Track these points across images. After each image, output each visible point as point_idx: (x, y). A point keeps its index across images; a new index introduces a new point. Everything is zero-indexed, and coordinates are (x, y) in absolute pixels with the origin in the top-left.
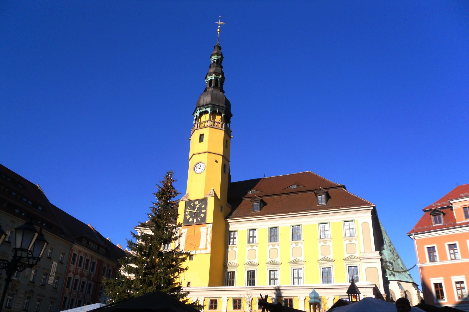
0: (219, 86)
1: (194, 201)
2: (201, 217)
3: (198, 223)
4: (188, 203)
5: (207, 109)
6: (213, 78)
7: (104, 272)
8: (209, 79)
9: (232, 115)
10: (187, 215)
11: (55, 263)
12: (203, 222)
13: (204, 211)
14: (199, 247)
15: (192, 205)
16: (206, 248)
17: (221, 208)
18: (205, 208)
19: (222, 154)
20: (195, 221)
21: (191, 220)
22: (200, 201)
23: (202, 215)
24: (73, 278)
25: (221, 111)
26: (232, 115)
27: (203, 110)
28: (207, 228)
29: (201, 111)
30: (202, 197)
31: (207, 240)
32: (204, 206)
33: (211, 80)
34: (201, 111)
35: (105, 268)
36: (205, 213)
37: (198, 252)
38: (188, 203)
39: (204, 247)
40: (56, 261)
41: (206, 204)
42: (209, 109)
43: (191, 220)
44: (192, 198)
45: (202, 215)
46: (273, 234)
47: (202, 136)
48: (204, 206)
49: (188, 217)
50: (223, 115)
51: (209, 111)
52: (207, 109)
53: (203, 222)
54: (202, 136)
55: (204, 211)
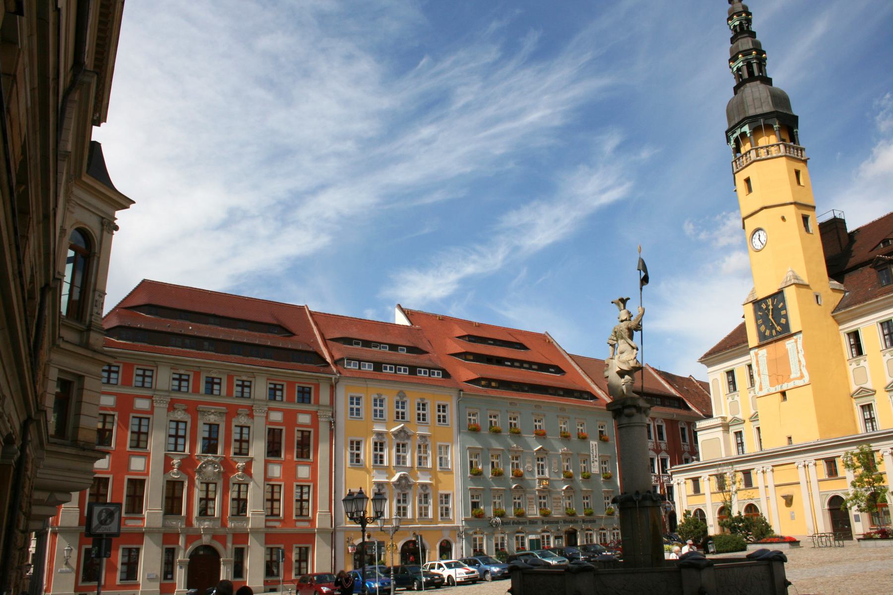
0: (756, 74)
3: (780, 336)
5: (743, 130)
7: (684, 436)
9: (797, 117)
11: (593, 443)
12: (785, 333)
13: (783, 312)
14: (792, 376)
15: (764, 306)
16: (802, 377)
17: (817, 297)
20: (774, 332)
21: (767, 333)
25: (770, 122)
26: (797, 117)
28: (796, 342)
29: (735, 135)
31: (799, 361)
34: (735, 135)
35: (683, 429)
39: (799, 375)
40: (594, 440)
41: (783, 300)
42: (746, 129)
43: (767, 333)
44: (760, 297)
45: (783, 321)
47: (748, 181)
49: (763, 328)
50: (776, 126)
51: (748, 131)
52: (743, 130)
54: (748, 181)
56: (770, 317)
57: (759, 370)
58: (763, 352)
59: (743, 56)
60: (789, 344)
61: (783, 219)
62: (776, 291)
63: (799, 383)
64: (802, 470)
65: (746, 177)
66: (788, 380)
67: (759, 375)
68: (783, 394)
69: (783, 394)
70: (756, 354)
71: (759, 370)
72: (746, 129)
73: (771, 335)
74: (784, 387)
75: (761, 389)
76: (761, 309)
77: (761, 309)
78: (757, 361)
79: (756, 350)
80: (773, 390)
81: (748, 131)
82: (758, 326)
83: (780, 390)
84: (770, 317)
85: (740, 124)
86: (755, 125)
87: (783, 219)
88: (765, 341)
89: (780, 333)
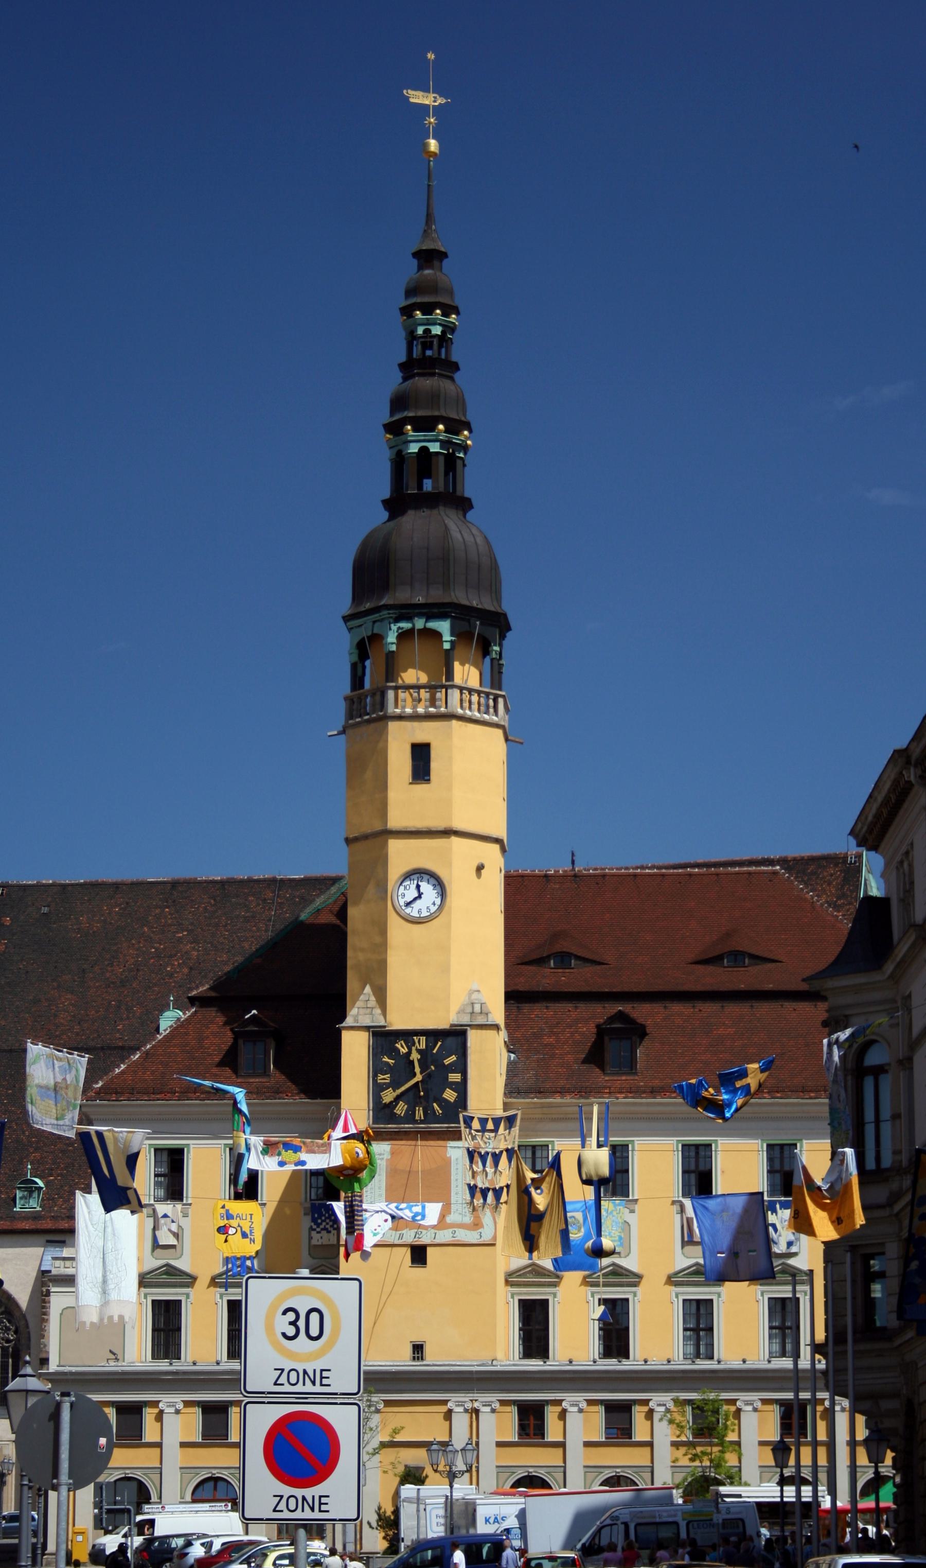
1: (408, 1035)
2: (443, 1103)
4: (384, 1039)
5: (433, 625)
6: (435, 448)
8: (414, 448)
13: (455, 1077)
19: (500, 830)
20: (419, 1113)
21: (401, 1109)
22: (433, 1035)
23: (450, 1095)
24: (424, 1363)
27: (420, 623)
29: (406, 625)
32: (453, 1058)
34: (406, 625)
36: (462, 1089)
38: (384, 1039)
43: (401, 1109)
44: (398, 1021)
45: (450, 1095)
48: (453, 1058)
52: (433, 625)
55: (455, 1077)
59: (447, 431)
61: (480, 868)
62: (443, 1025)
64: (461, 1422)
65: (420, 738)
69: (419, 1255)
72: (444, 627)
73: (410, 1117)
81: (447, 637)
82: (377, 1089)
87: (480, 868)
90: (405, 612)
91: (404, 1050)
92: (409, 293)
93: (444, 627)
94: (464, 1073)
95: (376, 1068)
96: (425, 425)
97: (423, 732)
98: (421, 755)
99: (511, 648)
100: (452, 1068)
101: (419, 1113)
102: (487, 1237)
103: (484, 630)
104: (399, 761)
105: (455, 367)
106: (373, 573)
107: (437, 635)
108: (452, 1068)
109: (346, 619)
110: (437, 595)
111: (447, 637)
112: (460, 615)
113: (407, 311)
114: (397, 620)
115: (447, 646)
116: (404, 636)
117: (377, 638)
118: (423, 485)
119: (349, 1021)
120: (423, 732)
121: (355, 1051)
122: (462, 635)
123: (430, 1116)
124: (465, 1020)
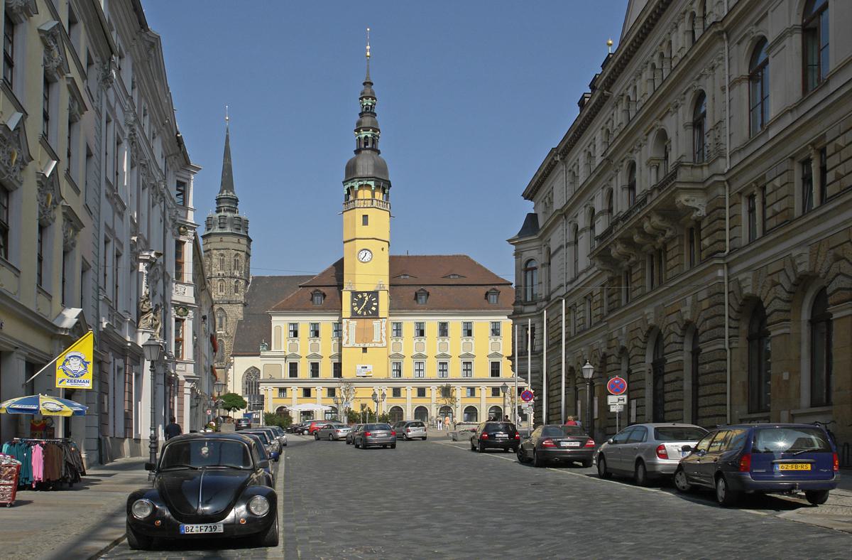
1: (361, 293)
4: (355, 294)
5: (369, 183)
6: (369, 136)
8: (363, 136)
10: (354, 306)
12: (375, 315)
16: (381, 342)
18: (377, 301)
20: (365, 313)
22: (369, 293)
27: (365, 182)
28: (381, 322)
29: (361, 183)
30: (372, 289)
33: (366, 137)
34: (361, 183)
36: (377, 307)
37: (372, 345)
38: (355, 294)
39: (379, 341)
44: (358, 290)
45: (374, 309)
46: (443, 330)
49: (356, 309)
52: (369, 183)
53: (375, 315)
56: (365, 304)
57: (348, 332)
58: (354, 323)
60: (376, 323)
61: (383, 249)
63: (377, 345)
66: (371, 341)
67: (348, 335)
68: (365, 350)
69: (365, 350)
70: (348, 322)
71: (348, 332)
72: (372, 183)
73: (362, 314)
74: (367, 345)
75: (347, 343)
76: (357, 297)
77: (357, 297)
78: (348, 327)
79: (348, 320)
80: (357, 345)
82: (353, 307)
83: (362, 345)
84: (365, 304)
85: (369, 178)
86: (378, 184)
87: (383, 249)
88: (355, 315)
89: (370, 315)
90: (361, 178)
91: (360, 297)
92: (361, 94)
93: (372, 183)
94: (378, 303)
95: (353, 301)
96: (366, 129)
97: (366, 212)
98: (365, 217)
99: (391, 191)
100: (374, 302)
101: (365, 313)
102: (384, 344)
103: (384, 185)
104: (360, 220)
105: (375, 115)
106: (351, 171)
107: (370, 186)
108: (374, 302)
109: (343, 182)
110: (370, 174)
111: (373, 186)
112: (377, 180)
113: (361, 99)
114: (360, 181)
115: (373, 189)
116: (361, 186)
117: (352, 187)
118: (368, 145)
119: (344, 289)
120: (366, 212)
121: (346, 296)
122: (377, 187)
123: (368, 314)
124: (378, 289)
